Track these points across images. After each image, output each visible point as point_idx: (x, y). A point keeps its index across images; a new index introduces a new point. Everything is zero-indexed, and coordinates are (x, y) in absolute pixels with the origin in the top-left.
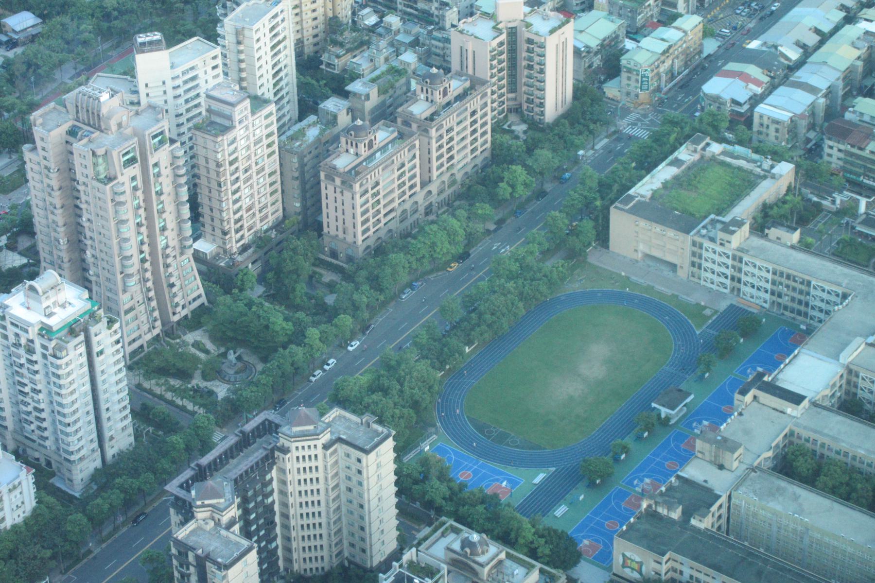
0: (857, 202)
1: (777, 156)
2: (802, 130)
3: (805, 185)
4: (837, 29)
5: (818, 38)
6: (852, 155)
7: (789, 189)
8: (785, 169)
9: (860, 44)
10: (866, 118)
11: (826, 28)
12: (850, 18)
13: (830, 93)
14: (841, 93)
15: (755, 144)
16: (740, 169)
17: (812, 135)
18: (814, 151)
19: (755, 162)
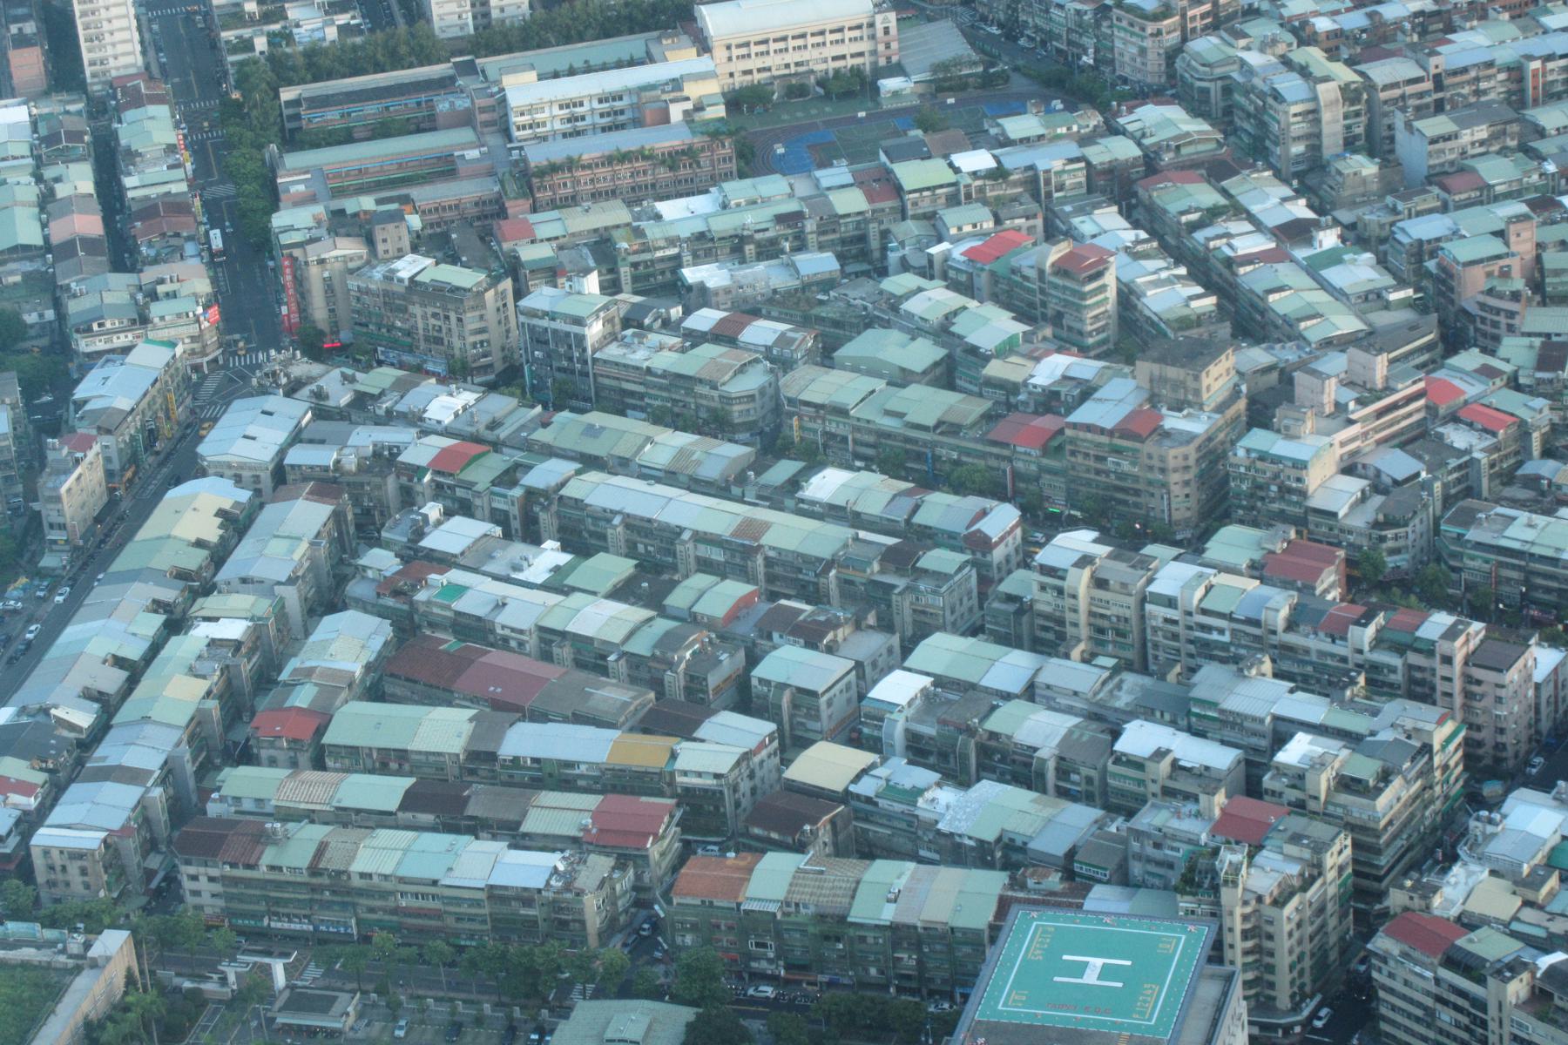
0: (267, 971)
1: (94, 923)
2: (132, 858)
3: (163, 962)
4: (155, 649)
5: (124, 674)
6: (235, 881)
7: (130, 980)
8: (113, 943)
9: (205, 667)
10: (248, 805)
11: (134, 652)
12: (176, 624)
13: (169, 772)
14: (190, 768)
15: (48, 907)
16: (25, 965)
17: (154, 862)
18: (166, 893)
19: (51, 944)
